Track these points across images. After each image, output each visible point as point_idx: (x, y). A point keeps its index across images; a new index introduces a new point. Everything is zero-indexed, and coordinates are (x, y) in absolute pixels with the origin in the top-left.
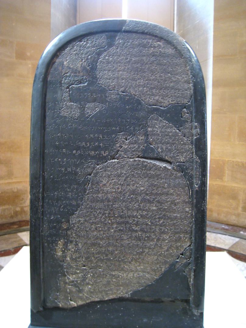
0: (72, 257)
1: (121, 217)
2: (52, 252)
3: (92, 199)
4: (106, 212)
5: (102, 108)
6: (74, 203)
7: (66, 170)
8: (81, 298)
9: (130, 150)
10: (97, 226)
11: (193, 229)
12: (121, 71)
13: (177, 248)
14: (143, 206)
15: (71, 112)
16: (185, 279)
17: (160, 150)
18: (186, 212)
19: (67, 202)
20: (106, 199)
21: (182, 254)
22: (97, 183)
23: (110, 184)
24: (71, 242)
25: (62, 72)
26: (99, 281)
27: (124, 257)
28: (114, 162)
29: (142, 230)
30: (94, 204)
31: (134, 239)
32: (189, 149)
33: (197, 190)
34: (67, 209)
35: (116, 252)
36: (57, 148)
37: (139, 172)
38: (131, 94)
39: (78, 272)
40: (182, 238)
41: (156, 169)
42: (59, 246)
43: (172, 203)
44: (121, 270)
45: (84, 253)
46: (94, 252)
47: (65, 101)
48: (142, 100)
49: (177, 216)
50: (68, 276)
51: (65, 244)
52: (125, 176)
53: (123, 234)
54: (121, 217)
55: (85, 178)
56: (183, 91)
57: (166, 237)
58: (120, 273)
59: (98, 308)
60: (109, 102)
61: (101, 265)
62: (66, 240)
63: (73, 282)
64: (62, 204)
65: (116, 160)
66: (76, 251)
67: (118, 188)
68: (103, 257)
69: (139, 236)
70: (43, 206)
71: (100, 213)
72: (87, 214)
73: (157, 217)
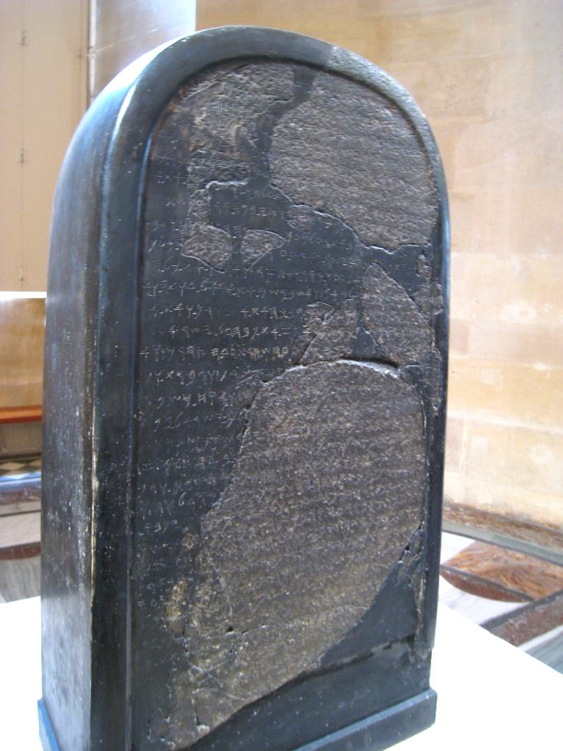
0: (204, 617)
1: (309, 494)
2: (156, 619)
3: (252, 463)
4: (279, 489)
5: (279, 244)
6: (212, 480)
7: (194, 400)
8: (223, 709)
9: (329, 342)
10: (260, 526)
11: (426, 494)
12: (320, 160)
14: (348, 463)
15: (209, 250)
16: (411, 594)
17: (381, 340)
18: (418, 462)
19: (195, 481)
20: (281, 458)
21: (407, 548)
22: (264, 425)
23: (291, 422)
24: (203, 579)
25: (188, 143)
26: (261, 654)
27: (311, 582)
28: (299, 372)
29: (346, 516)
30: (253, 477)
31: (331, 539)
32: (427, 335)
33: (436, 417)
34: (196, 499)
35: (297, 577)
36: (175, 342)
37: (345, 390)
38: (336, 216)
39: (218, 647)
40: (409, 516)
41: (373, 382)
42: (173, 598)
43: (396, 448)
44: (305, 614)
45: (231, 598)
47: (194, 219)
48: (355, 231)
49: (402, 473)
50: (195, 667)
51: (190, 592)
52: (319, 402)
53: (311, 532)
54: (309, 494)
55: (238, 416)
56: (421, 219)
57: (384, 519)
58: (303, 620)
59: (255, 717)
60: (294, 231)
61: (267, 615)
62: (191, 579)
63: (205, 675)
64: (182, 490)
65: (301, 367)
66: (214, 599)
67: (305, 431)
68: (272, 596)
69: (340, 530)
70: (134, 506)
71: (268, 493)
72: (240, 504)
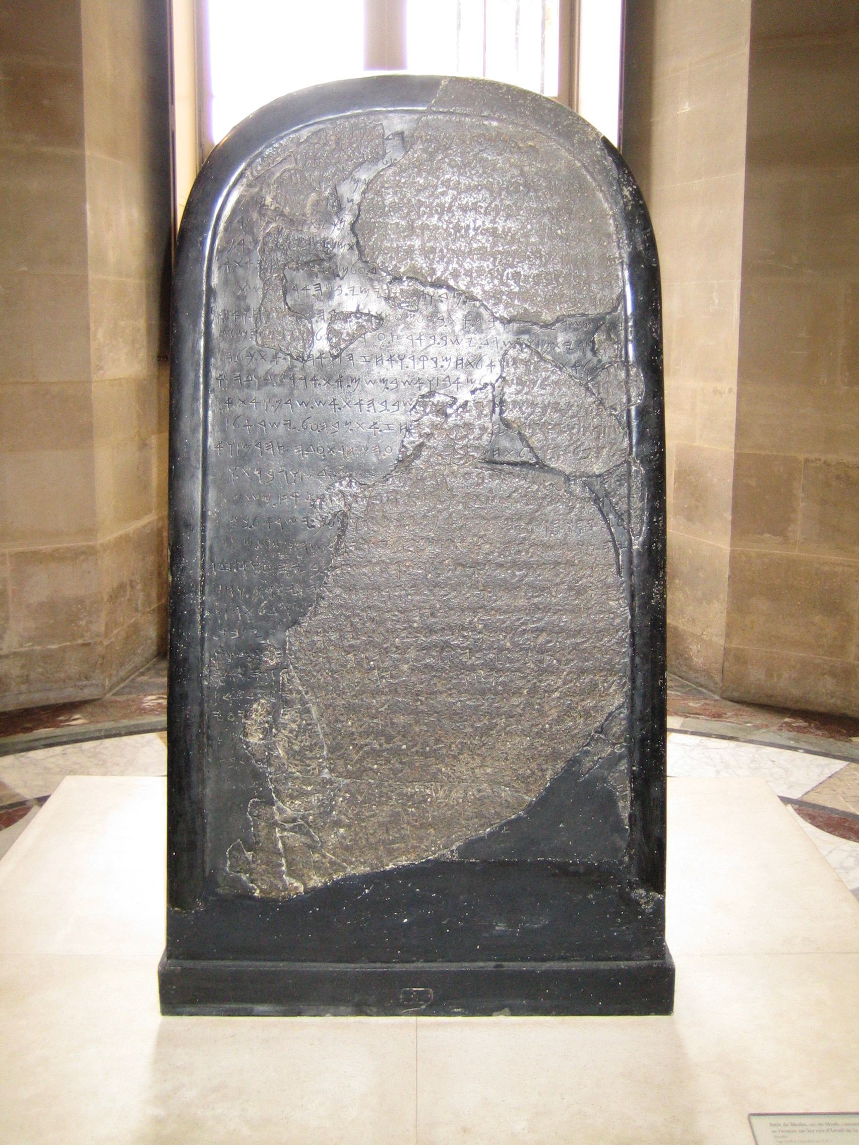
13: (587, 714)
39: (309, 788)
51: (274, 711)
66: (304, 730)
68: (381, 745)
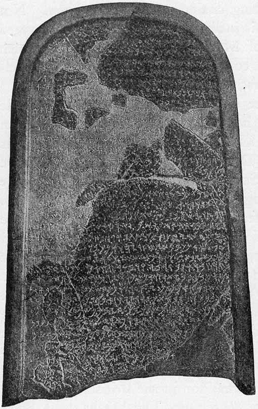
27: (138, 310)
46: (98, 305)
73: (181, 253)
